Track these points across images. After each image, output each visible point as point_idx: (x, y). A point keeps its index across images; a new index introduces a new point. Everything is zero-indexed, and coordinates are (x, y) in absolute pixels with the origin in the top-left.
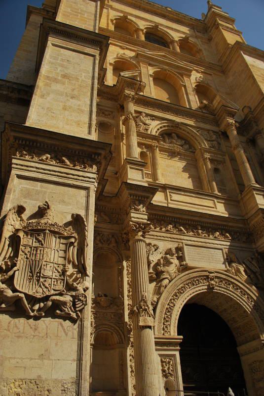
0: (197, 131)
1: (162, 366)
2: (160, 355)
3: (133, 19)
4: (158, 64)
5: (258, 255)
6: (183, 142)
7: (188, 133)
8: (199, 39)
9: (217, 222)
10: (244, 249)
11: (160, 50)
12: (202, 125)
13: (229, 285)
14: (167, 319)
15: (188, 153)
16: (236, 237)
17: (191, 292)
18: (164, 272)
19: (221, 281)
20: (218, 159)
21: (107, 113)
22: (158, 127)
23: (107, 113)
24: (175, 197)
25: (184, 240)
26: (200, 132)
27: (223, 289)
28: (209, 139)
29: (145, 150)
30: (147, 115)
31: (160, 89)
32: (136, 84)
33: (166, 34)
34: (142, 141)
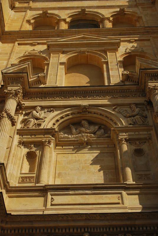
0: (114, 110)
3: (56, 12)
4: (74, 49)
6: (97, 127)
7: (101, 115)
8: (140, 7)
9: (114, 223)
11: (79, 33)
12: (120, 101)
15: (102, 140)
20: (142, 137)
22: (58, 118)
24: (58, 199)
26: (116, 110)
28: (128, 115)
29: (34, 149)
30: (43, 108)
31: (78, 74)
32: (22, 77)
33: (96, 14)
34: (30, 140)
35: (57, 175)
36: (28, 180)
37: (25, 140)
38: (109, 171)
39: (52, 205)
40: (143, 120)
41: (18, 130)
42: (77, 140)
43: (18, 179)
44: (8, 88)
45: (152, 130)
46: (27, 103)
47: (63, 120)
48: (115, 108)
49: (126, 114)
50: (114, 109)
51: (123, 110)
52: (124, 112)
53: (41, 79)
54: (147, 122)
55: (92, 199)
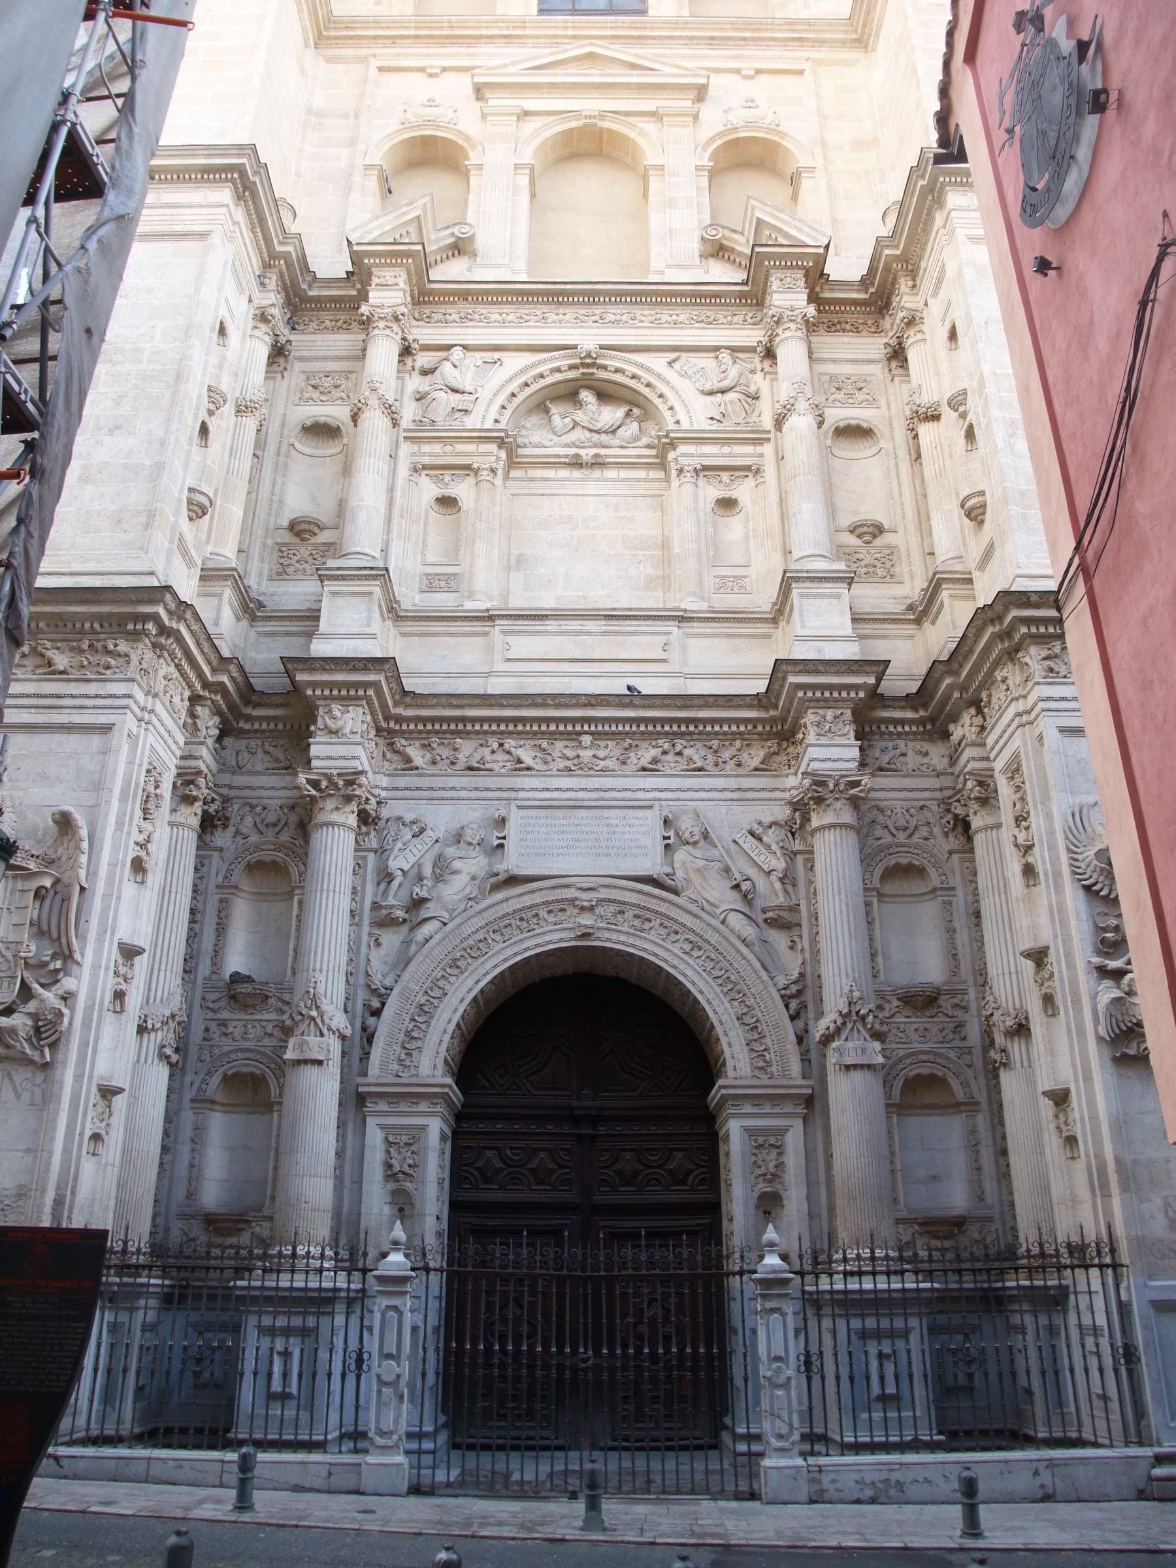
1: (388, 1152)
2: (382, 1127)
5: (795, 810)
6: (620, 412)
10: (750, 795)
13: (650, 920)
14: (415, 1034)
16: (726, 755)
17: (509, 952)
18: (424, 901)
19: (622, 912)
21: (327, 383)
22: (513, 387)
23: (327, 383)
24: (525, 645)
25: (523, 789)
26: (677, 365)
27: (622, 938)
28: (708, 387)
35: (513, 561)
36: (443, 584)
37: (427, 460)
38: (648, 553)
39: (509, 660)
40: (747, 407)
41: (405, 430)
42: (567, 456)
43: (417, 579)
44: (371, 295)
45: (769, 439)
46: (423, 334)
47: (528, 391)
48: (674, 361)
49: (703, 381)
50: (669, 363)
51: (694, 369)
52: (698, 375)
53: (461, 246)
54: (756, 414)
55: (601, 647)
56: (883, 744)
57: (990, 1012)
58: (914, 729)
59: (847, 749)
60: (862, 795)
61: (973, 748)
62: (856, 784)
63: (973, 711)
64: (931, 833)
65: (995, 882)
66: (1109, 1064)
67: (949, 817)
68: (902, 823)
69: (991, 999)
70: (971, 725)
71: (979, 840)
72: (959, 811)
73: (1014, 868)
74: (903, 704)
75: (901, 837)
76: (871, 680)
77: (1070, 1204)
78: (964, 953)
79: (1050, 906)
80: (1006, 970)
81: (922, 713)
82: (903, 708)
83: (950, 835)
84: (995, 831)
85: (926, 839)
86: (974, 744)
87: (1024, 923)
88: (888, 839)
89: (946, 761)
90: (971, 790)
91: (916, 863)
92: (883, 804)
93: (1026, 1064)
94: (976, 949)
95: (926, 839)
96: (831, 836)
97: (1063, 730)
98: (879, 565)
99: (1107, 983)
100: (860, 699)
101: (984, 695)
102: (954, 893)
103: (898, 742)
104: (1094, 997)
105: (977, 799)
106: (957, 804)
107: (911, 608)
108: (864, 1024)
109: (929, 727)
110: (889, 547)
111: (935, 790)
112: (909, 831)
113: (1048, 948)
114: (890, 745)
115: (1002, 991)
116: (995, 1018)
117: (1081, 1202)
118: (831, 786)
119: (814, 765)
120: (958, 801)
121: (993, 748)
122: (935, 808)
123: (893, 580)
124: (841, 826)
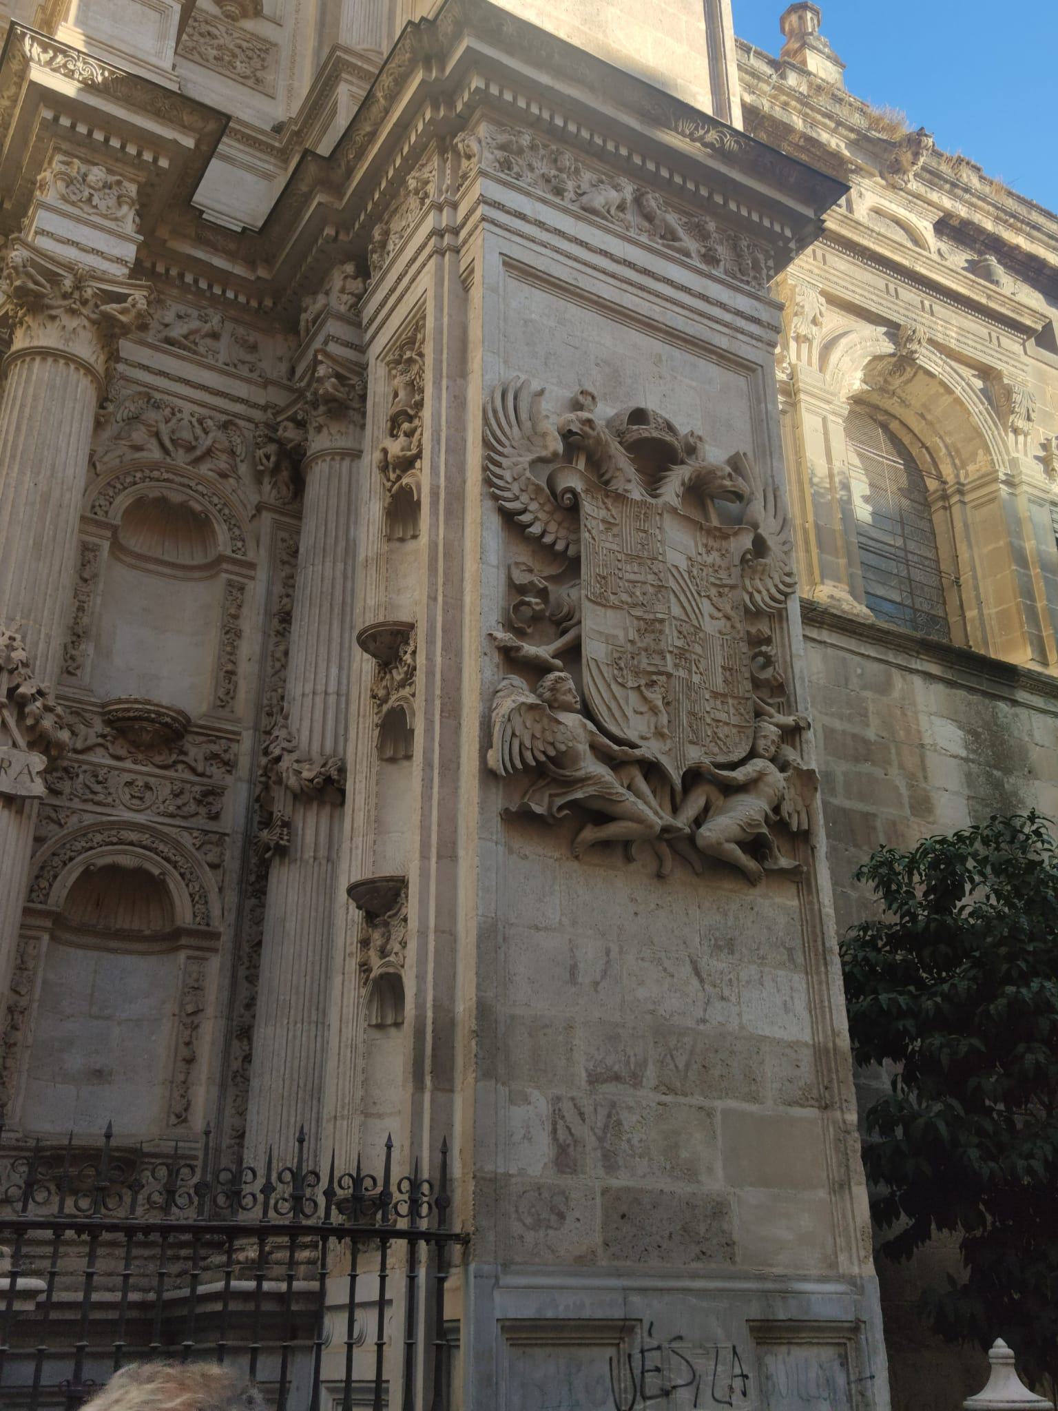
56: (182, 309)
57: (277, 752)
58: (242, 299)
59: (113, 240)
60: (123, 318)
61: (339, 323)
62: (121, 298)
63: (350, 268)
64: (234, 468)
65: (331, 541)
66: (496, 824)
67: (272, 448)
68: (186, 435)
69: (282, 733)
70: (343, 291)
71: (318, 477)
72: (290, 433)
73: (373, 510)
74: (232, 246)
75: (181, 458)
76: (189, 142)
77: (358, 1120)
78: (247, 669)
79: (433, 546)
80: (320, 688)
81: (262, 272)
82: (232, 256)
83: (266, 480)
84: (346, 463)
85: (224, 475)
86: (340, 317)
87: (371, 602)
88: (157, 454)
89: (284, 368)
90: (320, 380)
91: (198, 508)
92: (158, 396)
93: (322, 853)
94: (270, 671)
95: (224, 475)
96: (40, 370)
97: (511, 264)
98: (242, 57)
99: (517, 680)
100: (160, 172)
101: (377, 234)
102: (252, 573)
103: (210, 311)
104: (491, 696)
105: (329, 400)
106: (290, 425)
107: (278, 129)
108: (21, 717)
109: (268, 302)
110: (265, 41)
111: (255, 406)
112: (198, 453)
113: (412, 626)
114: (195, 313)
115: (306, 724)
116: (283, 765)
117: (380, 1116)
118: (68, 283)
119: (44, 243)
120: (292, 419)
121: (372, 320)
122: (249, 435)
123: (260, 88)
124: (70, 359)
